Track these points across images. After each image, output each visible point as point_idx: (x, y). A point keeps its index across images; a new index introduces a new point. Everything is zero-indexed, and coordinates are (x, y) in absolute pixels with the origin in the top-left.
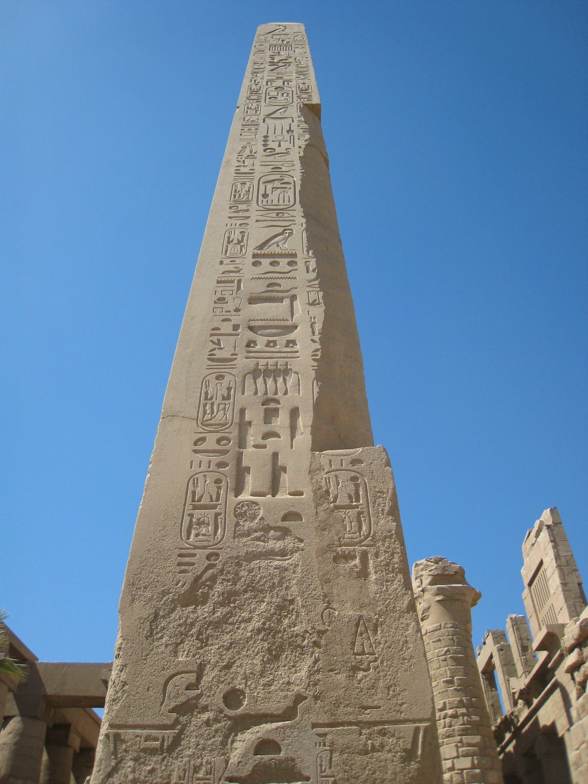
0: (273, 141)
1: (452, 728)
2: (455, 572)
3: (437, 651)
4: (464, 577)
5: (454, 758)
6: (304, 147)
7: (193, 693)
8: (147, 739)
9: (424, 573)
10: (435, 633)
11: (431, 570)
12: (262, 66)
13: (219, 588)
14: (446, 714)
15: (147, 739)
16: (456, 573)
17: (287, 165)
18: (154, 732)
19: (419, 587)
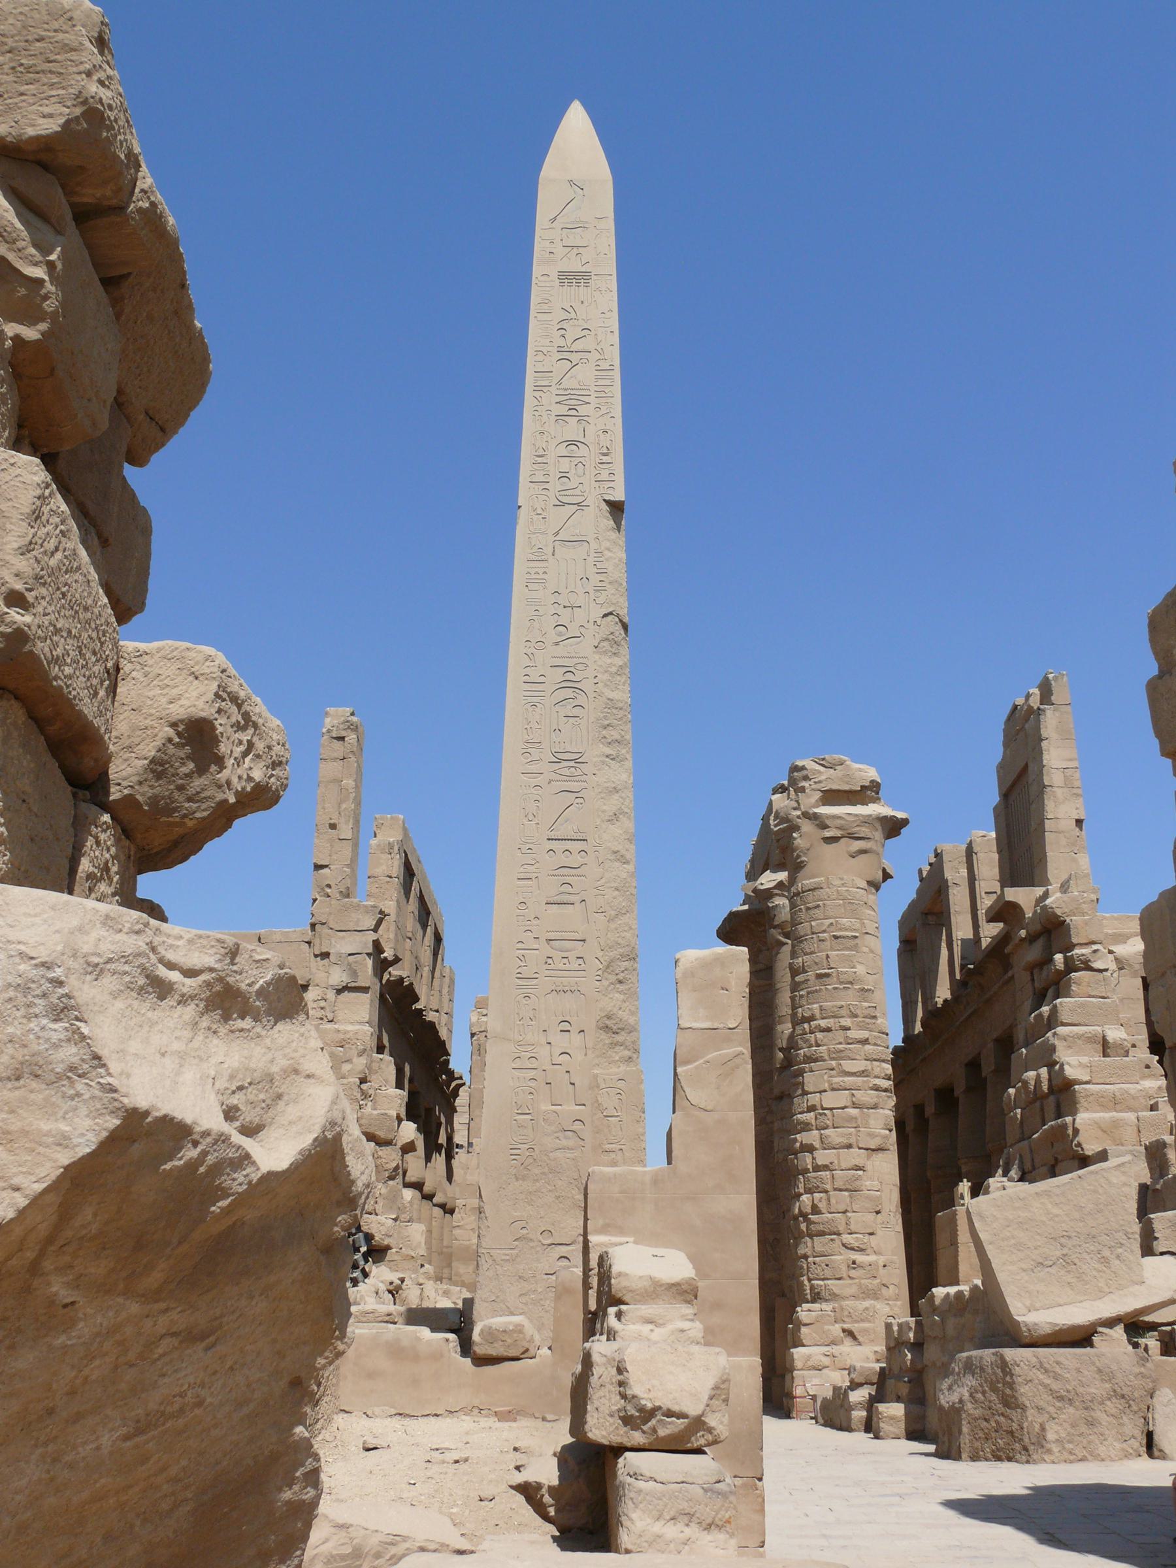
0: (565, 607)
2: (861, 787)
5: (820, 1092)
9: (805, 784)
10: (815, 893)
11: (820, 782)
17: (580, 667)
18: (507, 1252)
19: (795, 809)
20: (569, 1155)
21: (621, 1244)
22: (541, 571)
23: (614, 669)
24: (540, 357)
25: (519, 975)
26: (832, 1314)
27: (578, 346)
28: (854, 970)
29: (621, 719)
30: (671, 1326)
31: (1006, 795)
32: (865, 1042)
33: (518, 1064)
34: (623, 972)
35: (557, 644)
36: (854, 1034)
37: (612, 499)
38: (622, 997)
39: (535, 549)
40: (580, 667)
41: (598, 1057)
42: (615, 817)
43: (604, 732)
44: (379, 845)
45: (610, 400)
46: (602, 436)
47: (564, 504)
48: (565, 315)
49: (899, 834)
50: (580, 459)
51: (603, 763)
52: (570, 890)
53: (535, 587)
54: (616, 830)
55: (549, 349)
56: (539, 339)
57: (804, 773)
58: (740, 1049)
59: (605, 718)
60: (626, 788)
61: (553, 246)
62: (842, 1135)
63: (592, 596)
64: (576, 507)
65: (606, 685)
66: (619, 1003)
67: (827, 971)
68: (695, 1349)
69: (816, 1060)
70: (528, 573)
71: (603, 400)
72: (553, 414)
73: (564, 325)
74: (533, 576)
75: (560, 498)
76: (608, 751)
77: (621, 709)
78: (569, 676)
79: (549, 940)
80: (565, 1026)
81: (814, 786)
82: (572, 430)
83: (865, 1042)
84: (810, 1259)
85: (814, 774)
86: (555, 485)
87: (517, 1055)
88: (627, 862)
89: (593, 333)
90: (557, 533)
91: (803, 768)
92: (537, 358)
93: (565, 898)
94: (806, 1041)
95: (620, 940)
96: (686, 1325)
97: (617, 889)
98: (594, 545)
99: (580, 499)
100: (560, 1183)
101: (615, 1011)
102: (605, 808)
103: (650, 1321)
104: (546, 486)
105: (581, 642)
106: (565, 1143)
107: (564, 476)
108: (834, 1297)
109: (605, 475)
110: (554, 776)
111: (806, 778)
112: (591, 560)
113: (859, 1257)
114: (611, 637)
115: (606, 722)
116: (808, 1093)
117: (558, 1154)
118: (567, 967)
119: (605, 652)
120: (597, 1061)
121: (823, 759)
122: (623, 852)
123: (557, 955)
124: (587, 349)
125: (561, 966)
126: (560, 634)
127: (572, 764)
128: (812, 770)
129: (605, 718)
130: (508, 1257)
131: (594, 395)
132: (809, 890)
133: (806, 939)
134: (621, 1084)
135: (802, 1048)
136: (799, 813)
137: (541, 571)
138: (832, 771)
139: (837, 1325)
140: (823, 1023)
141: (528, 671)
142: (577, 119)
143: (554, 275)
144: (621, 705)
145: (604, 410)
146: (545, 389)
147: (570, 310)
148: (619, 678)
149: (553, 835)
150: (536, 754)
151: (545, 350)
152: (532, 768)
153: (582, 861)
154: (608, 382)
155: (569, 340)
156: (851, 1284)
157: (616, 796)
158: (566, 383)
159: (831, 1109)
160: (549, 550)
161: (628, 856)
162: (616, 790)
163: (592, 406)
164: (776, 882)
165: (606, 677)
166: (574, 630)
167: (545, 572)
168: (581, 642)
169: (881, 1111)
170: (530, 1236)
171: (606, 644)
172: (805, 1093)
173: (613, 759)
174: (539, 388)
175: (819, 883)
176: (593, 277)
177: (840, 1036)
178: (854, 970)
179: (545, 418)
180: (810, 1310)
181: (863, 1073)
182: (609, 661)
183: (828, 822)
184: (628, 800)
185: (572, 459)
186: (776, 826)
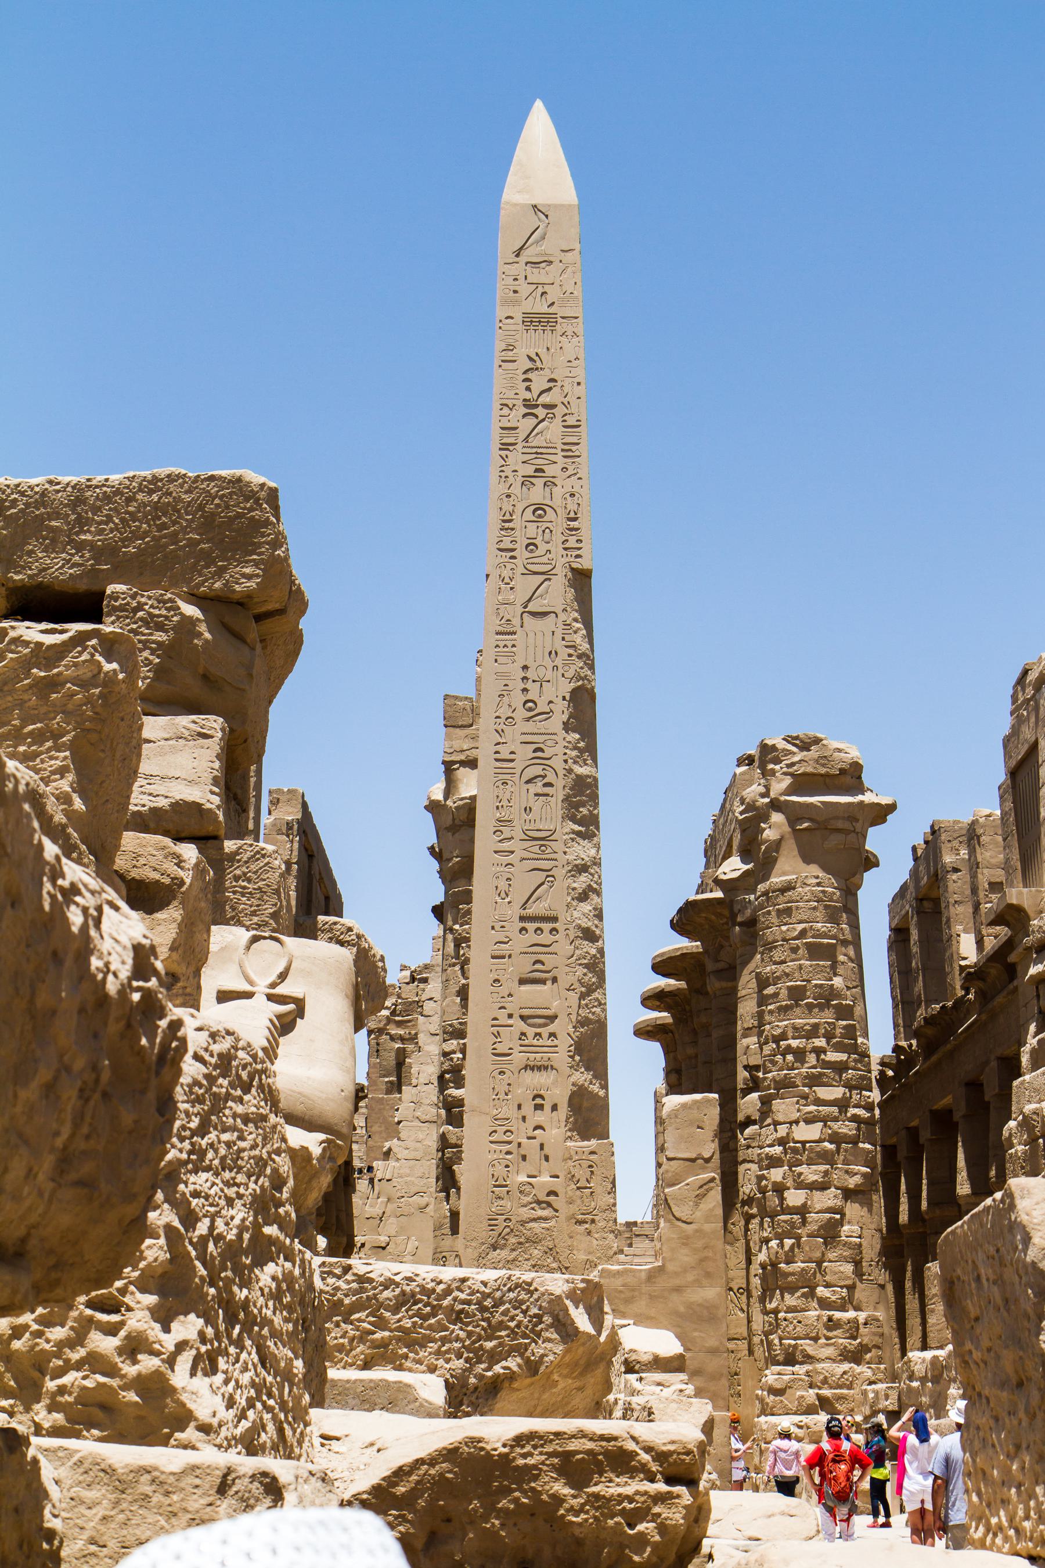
1: (796, 1071)
2: (840, 770)
3: (784, 928)
4: (860, 777)
5: (791, 1123)
11: (793, 764)
16: (843, 771)
19: (763, 796)
21: (625, 1326)
22: (510, 644)
24: (506, 411)
26: (807, 1378)
27: (545, 399)
28: (830, 983)
30: (673, 1388)
31: (1013, 774)
33: (495, 1137)
35: (528, 719)
36: (832, 1056)
40: (549, 743)
41: (570, 1130)
44: (274, 825)
45: (577, 460)
48: (530, 365)
49: (884, 821)
50: (549, 525)
51: (573, 840)
55: (514, 402)
56: (504, 390)
58: (713, 1174)
61: (516, 283)
62: (815, 1172)
63: (561, 671)
64: (543, 577)
65: (575, 762)
67: (799, 983)
68: (694, 1400)
70: (497, 646)
72: (520, 474)
73: (530, 375)
75: (528, 566)
76: (577, 828)
79: (522, 1017)
80: (539, 1101)
81: (785, 770)
82: (537, 493)
84: (781, 1315)
85: (786, 755)
86: (522, 554)
87: (494, 1129)
89: (559, 384)
92: (503, 412)
96: (684, 1387)
97: (586, 966)
98: (563, 616)
99: (549, 567)
100: (536, 1252)
102: (575, 885)
103: (659, 1384)
106: (540, 1213)
108: (809, 1359)
109: (572, 543)
111: (777, 761)
113: (837, 1315)
118: (541, 1042)
120: (569, 1134)
121: (797, 738)
123: (531, 1031)
125: (535, 1042)
126: (530, 710)
128: (784, 750)
131: (559, 451)
132: (779, 890)
133: (776, 947)
134: (593, 1157)
135: (770, 1071)
136: (767, 800)
137: (510, 644)
138: (805, 753)
139: (811, 1391)
140: (794, 1043)
143: (519, 318)
146: (511, 448)
147: (536, 358)
150: (507, 832)
151: (510, 403)
152: (506, 846)
154: (574, 440)
155: (535, 393)
156: (827, 1345)
159: (803, 1143)
160: (516, 621)
163: (559, 466)
164: (740, 872)
165: (575, 753)
167: (514, 646)
172: (776, 1123)
174: (505, 446)
175: (790, 882)
176: (560, 320)
178: (830, 983)
179: (511, 480)
180: (779, 1374)
185: (540, 524)
186: (741, 813)
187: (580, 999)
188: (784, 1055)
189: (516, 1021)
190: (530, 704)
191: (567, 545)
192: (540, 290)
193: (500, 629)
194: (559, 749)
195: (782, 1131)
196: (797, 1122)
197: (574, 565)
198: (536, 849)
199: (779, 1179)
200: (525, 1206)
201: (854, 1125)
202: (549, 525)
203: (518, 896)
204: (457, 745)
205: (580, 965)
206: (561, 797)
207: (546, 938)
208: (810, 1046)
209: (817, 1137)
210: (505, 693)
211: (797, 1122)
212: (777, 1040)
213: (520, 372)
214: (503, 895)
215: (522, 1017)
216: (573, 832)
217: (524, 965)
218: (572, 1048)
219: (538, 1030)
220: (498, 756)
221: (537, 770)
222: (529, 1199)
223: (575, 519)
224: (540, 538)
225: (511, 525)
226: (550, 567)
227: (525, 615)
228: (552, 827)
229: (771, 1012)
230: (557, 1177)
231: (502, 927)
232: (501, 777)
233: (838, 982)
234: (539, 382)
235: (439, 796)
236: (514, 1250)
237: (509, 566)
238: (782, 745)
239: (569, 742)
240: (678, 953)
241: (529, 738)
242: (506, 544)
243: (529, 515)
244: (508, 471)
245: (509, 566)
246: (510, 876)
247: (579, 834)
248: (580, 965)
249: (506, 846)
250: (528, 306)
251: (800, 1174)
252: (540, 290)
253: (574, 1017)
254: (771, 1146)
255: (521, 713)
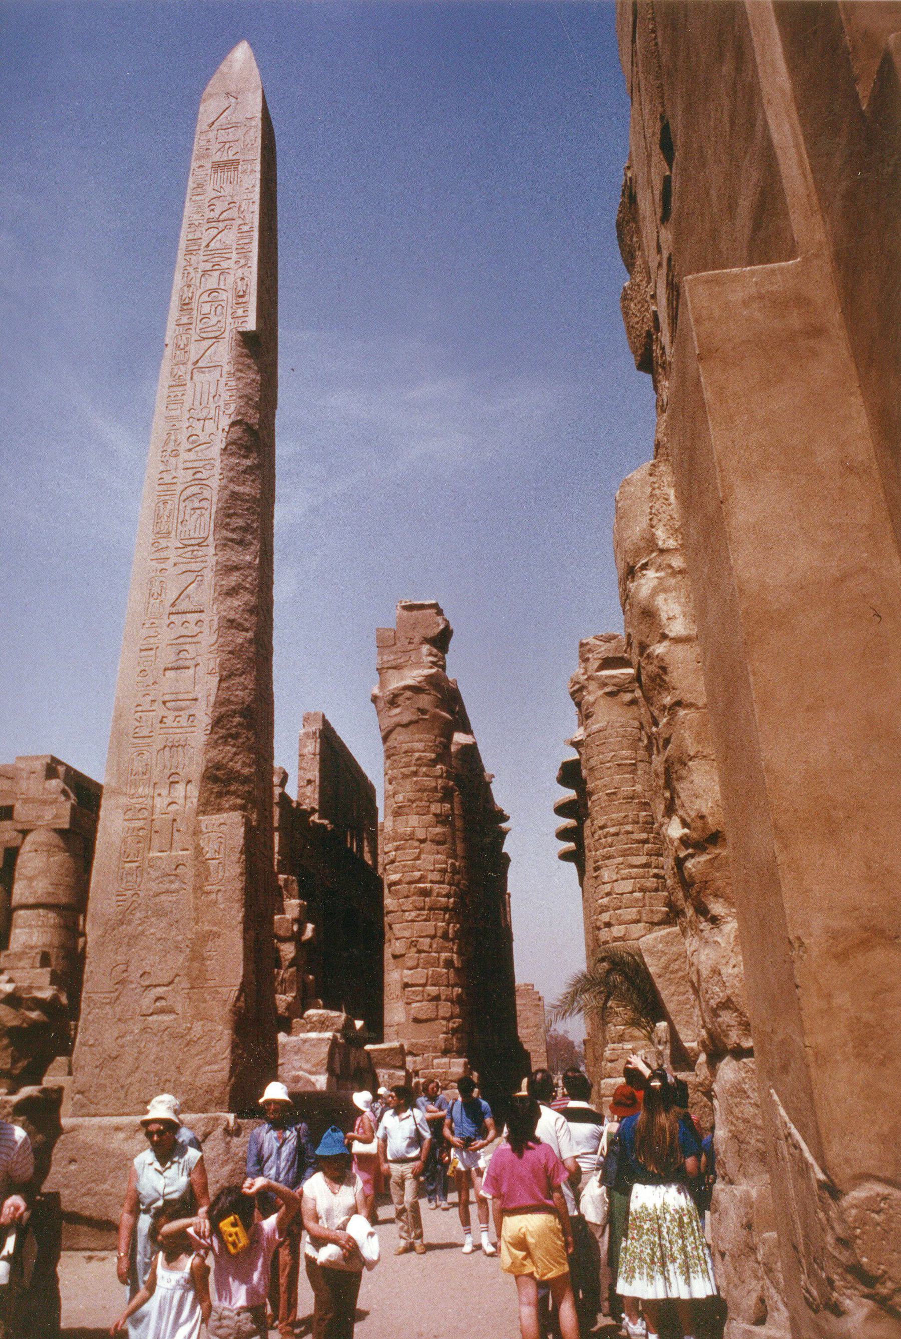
3: (601, 756)
5: (613, 882)
6: (227, 429)
7: (125, 975)
8: (105, 998)
9: (590, 656)
12: (198, 235)
13: (138, 915)
14: (608, 833)
15: (105, 998)
18: (107, 995)
19: (583, 674)
20: (170, 899)
22: (180, 394)
23: (241, 468)
25: (136, 735)
29: (247, 510)
32: (646, 841)
34: (236, 727)
35: (190, 450)
37: (244, 330)
38: (234, 749)
39: (177, 377)
40: (208, 467)
42: (232, 592)
43: (228, 520)
46: (239, 283)
47: (204, 339)
51: (225, 545)
52: (188, 656)
53: (173, 407)
54: (236, 602)
57: (588, 647)
59: (229, 508)
60: (249, 567)
63: (222, 409)
64: (214, 340)
66: (230, 755)
69: (609, 858)
71: (242, 255)
73: (213, 202)
74: (173, 398)
75: (202, 335)
77: (248, 501)
78: (198, 476)
79: (164, 703)
80: (174, 778)
81: (596, 656)
82: (212, 282)
83: (646, 841)
88: (246, 630)
90: (197, 362)
91: (587, 644)
93: (181, 663)
94: (600, 844)
95: (232, 698)
97: (230, 652)
101: (225, 761)
102: (223, 583)
104: (191, 326)
105: (209, 447)
107: (205, 316)
110: (181, 560)
111: (590, 651)
112: (223, 381)
114: (239, 442)
115: (231, 511)
116: (604, 883)
117: (162, 898)
119: (233, 454)
122: (241, 621)
123: (171, 715)
124: (230, 217)
127: (196, 548)
129: (229, 508)
130: (108, 1001)
131: (235, 252)
136: (586, 677)
137: (180, 394)
141: (164, 475)
142: (242, 53)
143: (208, 165)
144: (248, 498)
145: (242, 262)
146: (194, 253)
148: (247, 476)
149: (174, 610)
152: (162, 555)
153: (198, 629)
157: (236, 574)
158: (212, 246)
159: (622, 894)
161: (247, 625)
162: (236, 568)
163: (234, 260)
166: (203, 438)
168: (209, 447)
169: (660, 893)
170: (130, 979)
171: (233, 447)
173: (238, 543)
174: (189, 252)
176: (241, 163)
177: (623, 837)
181: (647, 865)
182: (237, 461)
183: (606, 681)
184: (250, 579)
187: (220, 681)
188: (605, 837)
189: (157, 706)
190: (194, 438)
191: (237, 315)
192: (227, 146)
193: (174, 383)
194: (217, 471)
195: (607, 888)
196: (617, 881)
197: (240, 329)
198: (189, 555)
199: (607, 920)
200: (154, 881)
201: (654, 880)
202: (221, 303)
203: (171, 595)
204: (385, 658)
205: (223, 651)
206: (214, 510)
207: (192, 629)
208: (623, 830)
209: (630, 889)
210: (172, 432)
211: (617, 881)
212: (602, 828)
213: (206, 201)
214: (156, 596)
215: (164, 703)
216: (226, 539)
217: (168, 657)
218: (209, 728)
219: (177, 713)
220: (162, 481)
221: (195, 490)
222: (158, 874)
223: (242, 296)
224: (213, 313)
225: (189, 307)
226: (219, 333)
227: (195, 370)
228: (205, 535)
229: (596, 811)
230: (187, 850)
231: (153, 623)
232: (162, 498)
233: (638, 788)
234: (220, 206)
235: (376, 691)
236: (140, 925)
237: (184, 336)
238: (591, 640)
239: (226, 465)
240: (566, 801)
241: (191, 465)
242: (185, 320)
243: (205, 297)
244: (190, 269)
245: (184, 336)
246: (163, 579)
247: (232, 540)
248: (223, 651)
249: (162, 555)
250: (216, 158)
251: (621, 915)
252: (227, 146)
253: (212, 699)
254: (602, 898)
255: (185, 445)
